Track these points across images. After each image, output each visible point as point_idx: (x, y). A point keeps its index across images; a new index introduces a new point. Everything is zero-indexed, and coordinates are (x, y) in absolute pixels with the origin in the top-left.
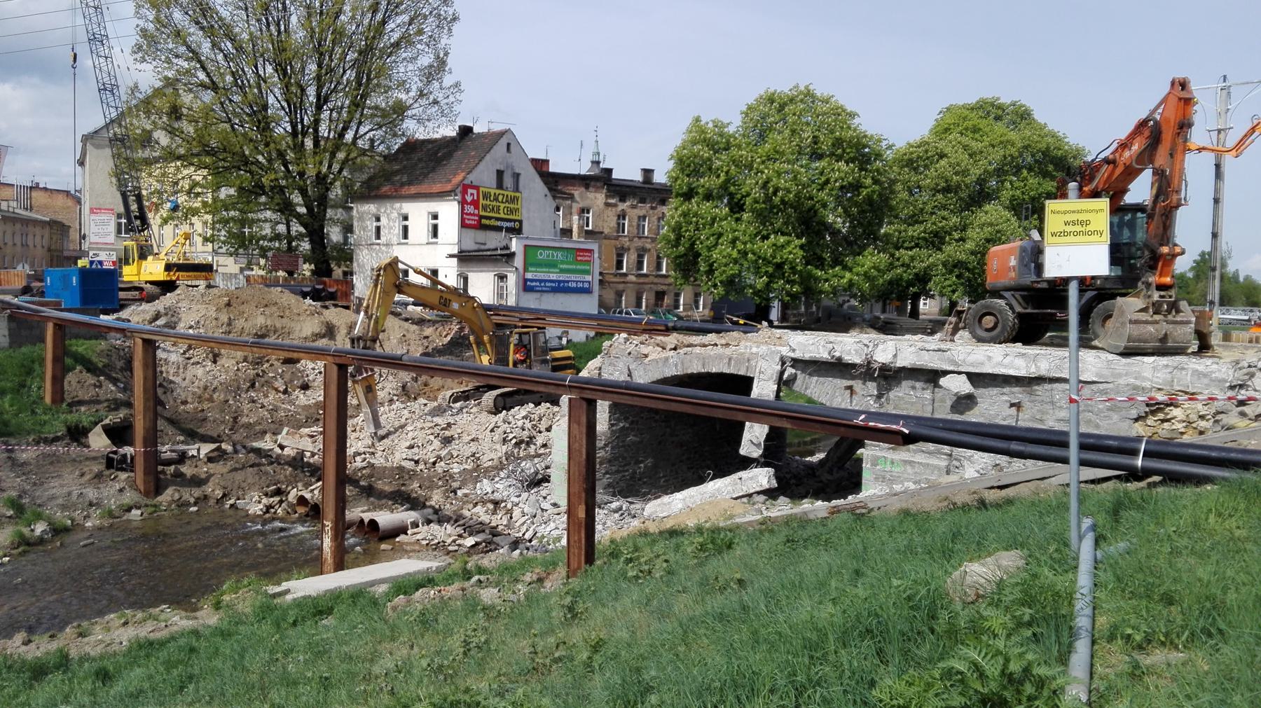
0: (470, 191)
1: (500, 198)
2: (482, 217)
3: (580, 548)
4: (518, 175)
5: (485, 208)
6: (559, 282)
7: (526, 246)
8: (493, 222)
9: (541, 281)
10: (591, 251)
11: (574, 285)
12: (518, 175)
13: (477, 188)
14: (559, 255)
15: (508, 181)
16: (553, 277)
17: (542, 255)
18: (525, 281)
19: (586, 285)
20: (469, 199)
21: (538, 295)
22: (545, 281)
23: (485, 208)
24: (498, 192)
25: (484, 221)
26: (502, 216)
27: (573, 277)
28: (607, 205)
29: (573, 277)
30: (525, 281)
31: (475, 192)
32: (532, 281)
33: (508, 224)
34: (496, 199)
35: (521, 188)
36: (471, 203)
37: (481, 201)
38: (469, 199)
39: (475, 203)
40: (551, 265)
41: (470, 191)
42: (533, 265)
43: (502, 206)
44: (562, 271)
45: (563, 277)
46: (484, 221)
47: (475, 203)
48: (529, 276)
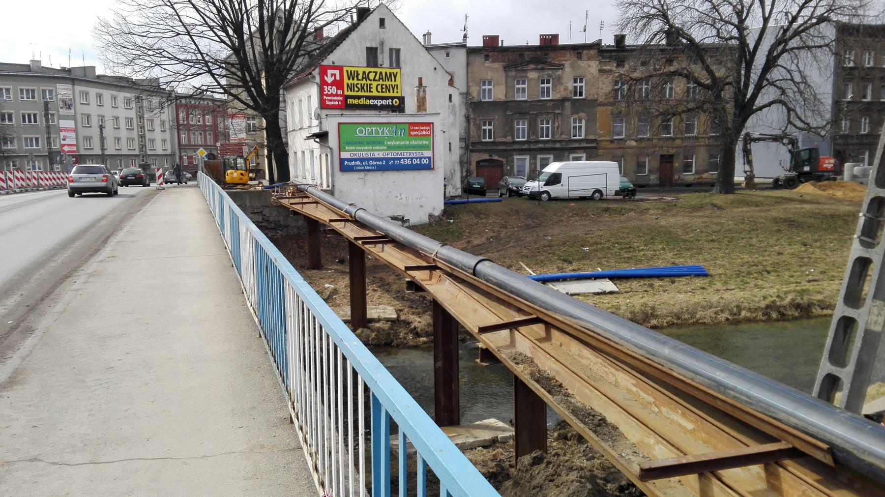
0: (330, 72)
1: (372, 76)
2: (347, 97)
3: (692, 380)
4: (398, 51)
6: (387, 160)
7: (339, 124)
8: (362, 101)
9: (362, 160)
11: (409, 162)
12: (398, 51)
13: (340, 68)
15: (384, 58)
18: (342, 161)
19: (425, 161)
20: (329, 79)
21: (362, 175)
22: (368, 160)
23: (351, 88)
24: (367, 70)
25: (350, 101)
26: (375, 94)
27: (406, 154)
28: (601, 71)
29: (406, 154)
30: (342, 161)
31: (337, 72)
33: (384, 102)
35: (402, 64)
36: (332, 84)
37: (346, 80)
38: (329, 79)
39: (338, 84)
41: (330, 72)
43: (375, 84)
44: (390, 148)
45: (392, 154)
46: (350, 101)
47: (338, 84)
48: (345, 155)
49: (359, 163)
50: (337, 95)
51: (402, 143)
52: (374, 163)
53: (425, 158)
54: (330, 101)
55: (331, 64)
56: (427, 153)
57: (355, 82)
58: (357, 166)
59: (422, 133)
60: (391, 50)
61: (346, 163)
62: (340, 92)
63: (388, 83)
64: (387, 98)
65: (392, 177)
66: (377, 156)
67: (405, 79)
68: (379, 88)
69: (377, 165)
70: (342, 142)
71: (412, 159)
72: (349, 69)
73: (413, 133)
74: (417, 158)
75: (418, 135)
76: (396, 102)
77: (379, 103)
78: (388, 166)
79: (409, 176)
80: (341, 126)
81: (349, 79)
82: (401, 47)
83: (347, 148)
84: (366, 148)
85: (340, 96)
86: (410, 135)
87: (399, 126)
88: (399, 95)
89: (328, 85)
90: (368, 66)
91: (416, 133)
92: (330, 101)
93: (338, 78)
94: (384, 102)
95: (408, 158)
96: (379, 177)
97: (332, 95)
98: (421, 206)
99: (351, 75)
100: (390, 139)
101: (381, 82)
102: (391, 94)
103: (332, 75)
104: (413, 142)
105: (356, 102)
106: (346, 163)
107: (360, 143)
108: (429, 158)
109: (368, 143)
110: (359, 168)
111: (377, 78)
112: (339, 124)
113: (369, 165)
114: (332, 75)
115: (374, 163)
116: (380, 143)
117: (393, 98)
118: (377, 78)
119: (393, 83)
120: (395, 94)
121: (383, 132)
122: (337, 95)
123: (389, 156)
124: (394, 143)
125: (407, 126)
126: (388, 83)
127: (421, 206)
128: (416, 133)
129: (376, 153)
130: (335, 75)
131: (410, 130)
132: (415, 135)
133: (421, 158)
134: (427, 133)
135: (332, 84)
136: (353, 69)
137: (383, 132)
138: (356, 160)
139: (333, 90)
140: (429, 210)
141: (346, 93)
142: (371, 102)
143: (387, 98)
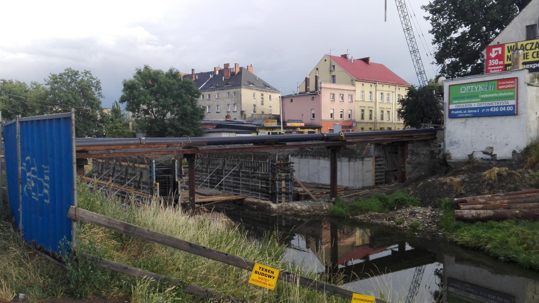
1: (528, 47)
6: (481, 108)
7: (450, 86)
9: (463, 110)
11: (496, 110)
13: (502, 46)
18: (450, 111)
19: (510, 109)
20: (493, 55)
21: (463, 120)
22: (467, 109)
26: (531, 59)
31: (500, 49)
32: (455, 110)
37: (506, 53)
39: (500, 57)
42: (455, 99)
43: (531, 52)
44: (483, 100)
48: (452, 107)
49: (461, 112)
50: (499, 65)
51: (492, 95)
52: (471, 111)
53: (510, 106)
54: (493, 70)
55: (497, 44)
56: (512, 102)
58: (459, 114)
59: (508, 86)
61: (452, 112)
62: (501, 63)
66: (473, 106)
68: (535, 55)
69: (473, 113)
70: (451, 97)
71: (499, 107)
72: (509, 45)
73: (500, 87)
74: (503, 106)
75: (504, 89)
78: (482, 113)
79: (498, 120)
80: (451, 87)
81: (509, 52)
83: (454, 102)
84: (466, 101)
85: (501, 65)
86: (498, 89)
87: (490, 82)
89: (492, 59)
90: (528, 39)
91: (503, 87)
92: (493, 70)
93: (500, 53)
95: (496, 107)
97: (495, 66)
98: (507, 145)
100: (483, 93)
103: (496, 52)
104: (500, 94)
106: (452, 112)
107: (462, 98)
108: (514, 106)
109: (468, 97)
110: (460, 115)
111: (534, 47)
112: (450, 86)
113: (468, 113)
114: (496, 52)
115: (471, 111)
116: (476, 97)
118: (534, 47)
121: (478, 89)
122: (499, 65)
123: (482, 106)
125: (496, 83)
127: (507, 145)
128: (503, 87)
129: (473, 104)
130: (498, 51)
131: (499, 85)
132: (502, 89)
133: (506, 106)
134: (512, 86)
135: (495, 58)
137: (478, 89)
138: (459, 110)
139: (496, 62)
140: (513, 148)
141: (506, 63)
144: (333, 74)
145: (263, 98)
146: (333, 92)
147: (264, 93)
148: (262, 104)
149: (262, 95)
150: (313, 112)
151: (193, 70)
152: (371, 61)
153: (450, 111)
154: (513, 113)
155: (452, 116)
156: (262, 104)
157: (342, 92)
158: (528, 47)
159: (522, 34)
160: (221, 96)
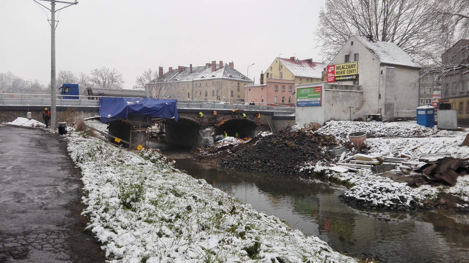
1: (345, 67)
5: (337, 73)
6: (308, 102)
8: (341, 78)
9: (302, 102)
10: (321, 87)
11: (314, 103)
13: (334, 66)
14: (308, 91)
15: (352, 59)
16: (306, 100)
17: (303, 92)
18: (297, 102)
19: (318, 102)
20: (330, 71)
21: (302, 108)
23: (337, 73)
25: (337, 79)
26: (346, 74)
27: (313, 99)
29: (313, 99)
31: (333, 67)
32: (299, 102)
33: (349, 78)
34: (343, 68)
36: (331, 73)
37: (336, 70)
39: (333, 72)
40: (305, 95)
42: (300, 96)
43: (346, 70)
44: (310, 97)
45: (309, 100)
48: (298, 100)
50: (332, 77)
57: (339, 70)
60: (355, 55)
62: (333, 75)
63: (351, 69)
64: (350, 76)
65: (310, 109)
67: (359, 66)
72: (337, 65)
76: (354, 77)
77: (347, 78)
78: (309, 105)
82: (359, 52)
88: (356, 74)
89: (329, 73)
94: (349, 78)
96: (306, 108)
97: (331, 77)
99: (338, 68)
100: (309, 94)
101: (349, 69)
102: (353, 74)
105: (338, 79)
116: (306, 95)
117: (353, 75)
119: (354, 69)
120: (355, 74)
122: (332, 77)
124: (310, 95)
126: (351, 69)
136: (338, 65)
142: (344, 78)
143: (350, 76)
144: (281, 71)
145: (239, 86)
146: (276, 85)
147: (240, 83)
148: (239, 90)
149: (239, 84)
150: (263, 98)
151: (191, 65)
152: (313, 61)
153: (297, 102)
154: (320, 105)
155: (298, 106)
156: (239, 90)
157: (284, 85)
158: (345, 67)
159: (343, 59)
160: (208, 84)
